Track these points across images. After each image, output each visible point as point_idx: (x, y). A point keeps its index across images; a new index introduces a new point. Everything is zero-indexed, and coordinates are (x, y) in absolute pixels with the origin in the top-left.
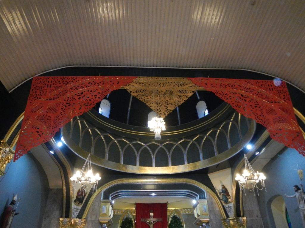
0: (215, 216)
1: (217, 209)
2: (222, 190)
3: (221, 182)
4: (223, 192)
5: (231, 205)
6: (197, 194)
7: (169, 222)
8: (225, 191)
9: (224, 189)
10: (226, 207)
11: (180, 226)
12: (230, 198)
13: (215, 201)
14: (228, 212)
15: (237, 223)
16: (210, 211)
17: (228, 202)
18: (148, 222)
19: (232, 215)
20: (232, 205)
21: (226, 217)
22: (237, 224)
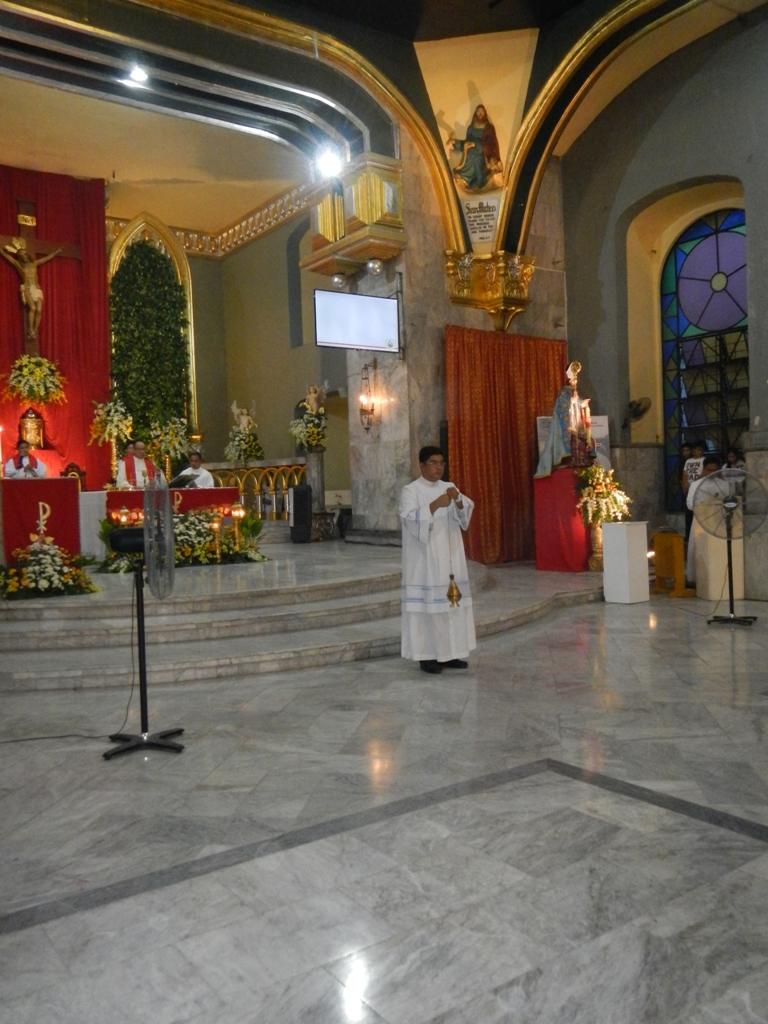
0: (425, 238)
1: (435, 210)
2: (471, 128)
3: (473, 90)
4: (470, 138)
5: (491, 205)
6: (359, 124)
7: (113, 268)
8: (482, 136)
9: (482, 126)
10: (471, 206)
11: (170, 286)
12: (500, 171)
13: (429, 175)
14: (470, 231)
15: (505, 275)
16: (411, 212)
17: (490, 183)
18: (15, 251)
19: (486, 244)
20: (498, 203)
21: (463, 249)
22: (502, 279)
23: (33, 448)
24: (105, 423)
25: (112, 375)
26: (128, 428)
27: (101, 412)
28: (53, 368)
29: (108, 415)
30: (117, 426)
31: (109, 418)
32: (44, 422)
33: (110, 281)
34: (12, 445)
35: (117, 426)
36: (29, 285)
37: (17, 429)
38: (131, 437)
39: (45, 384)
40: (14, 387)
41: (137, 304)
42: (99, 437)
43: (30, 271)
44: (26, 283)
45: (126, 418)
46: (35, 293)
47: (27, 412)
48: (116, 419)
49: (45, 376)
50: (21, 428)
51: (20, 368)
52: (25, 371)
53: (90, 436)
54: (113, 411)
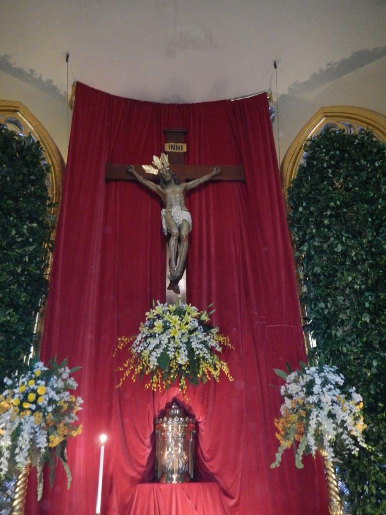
18: (155, 172)
23: (175, 477)
24: (304, 412)
25: (307, 328)
26: (356, 419)
27: (293, 388)
28: (205, 318)
29: (309, 393)
30: (331, 416)
31: (312, 399)
32: (196, 424)
33: (287, 196)
34: (133, 473)
35: (331, 416)
36: (171, 206)
37: (148, 441)
38: (367, 441)
39: (189, 343)
40: (139, 355)
41: (332, 204)
42: (297, 443)
43: (174, 193)
44: (168, 207)
45: (349, 397)
46: (178, 215)
47: (169, 406)
48: (327, 398)
49: (191, 332)
50: (157, 441)
51: (152, 327)
52: (159, 324)
53: (278, 444)
54: (318, 381)
